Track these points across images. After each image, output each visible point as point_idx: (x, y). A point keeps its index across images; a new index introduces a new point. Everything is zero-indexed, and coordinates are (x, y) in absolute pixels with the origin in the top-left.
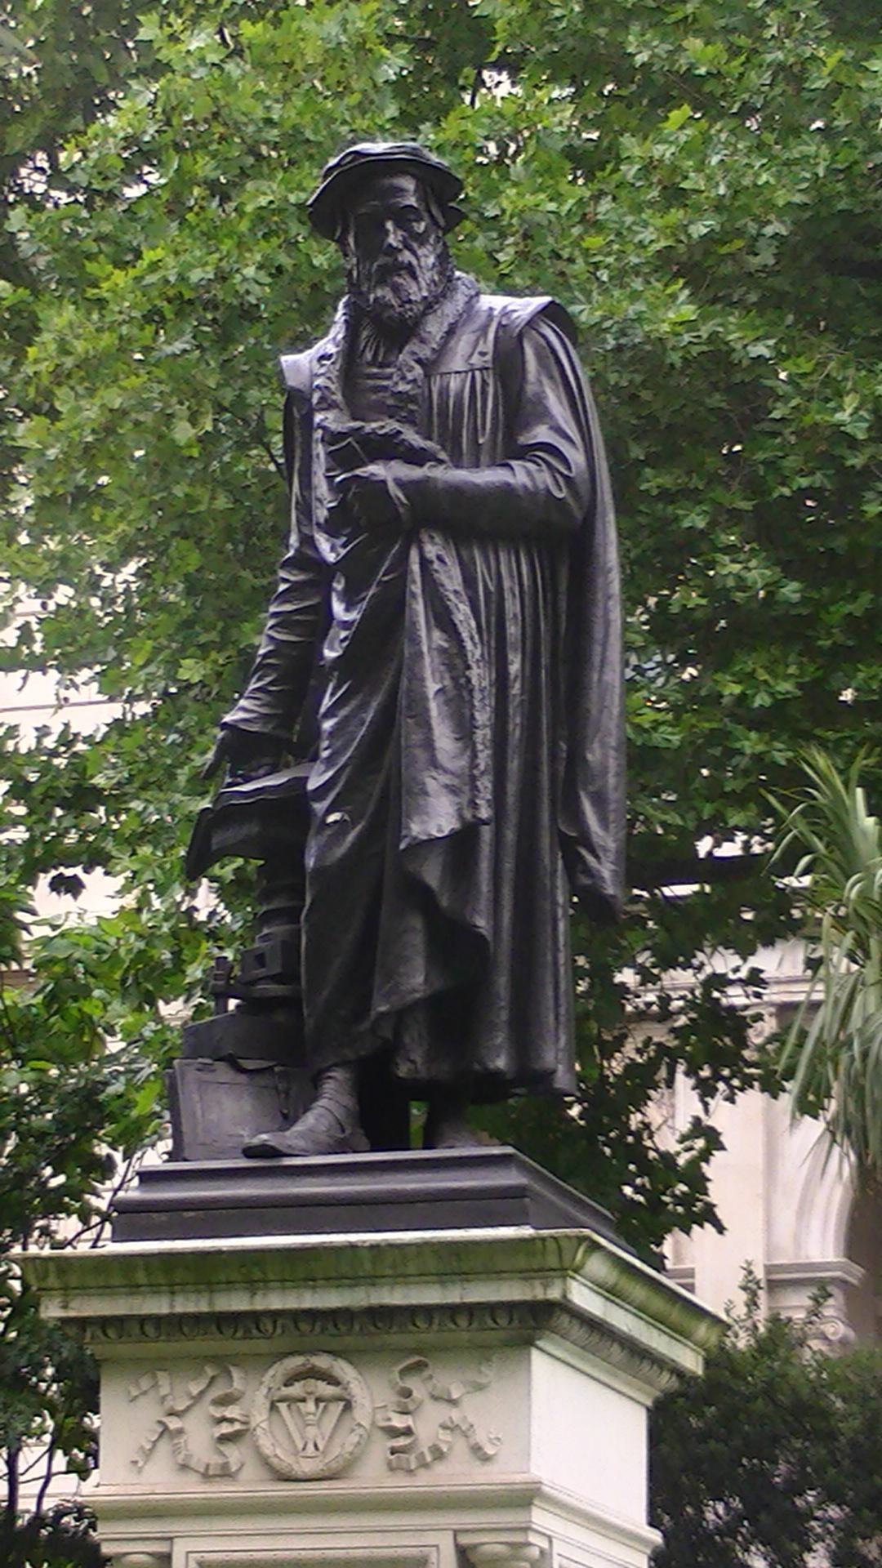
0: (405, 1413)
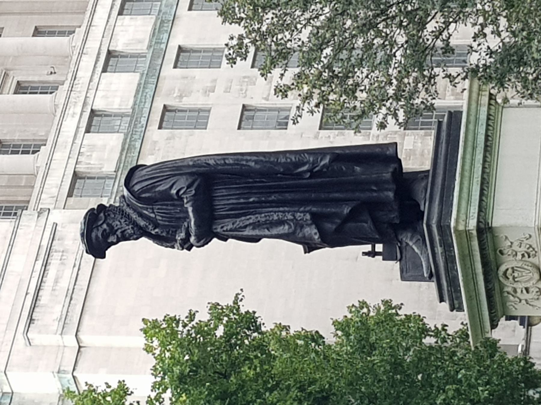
0: (516, 255)
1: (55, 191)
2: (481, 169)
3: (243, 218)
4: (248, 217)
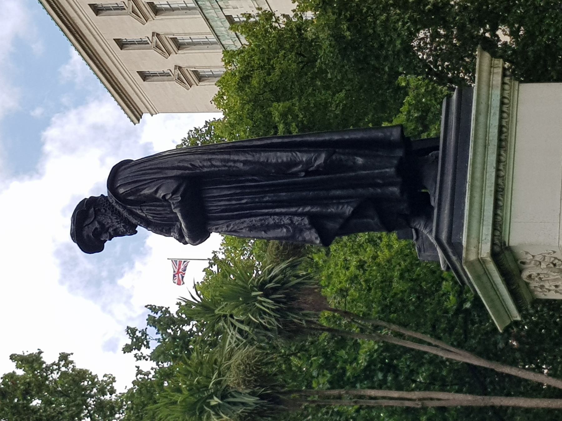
2: (494, 174)
3: (238, 221)
4: (242, 220)
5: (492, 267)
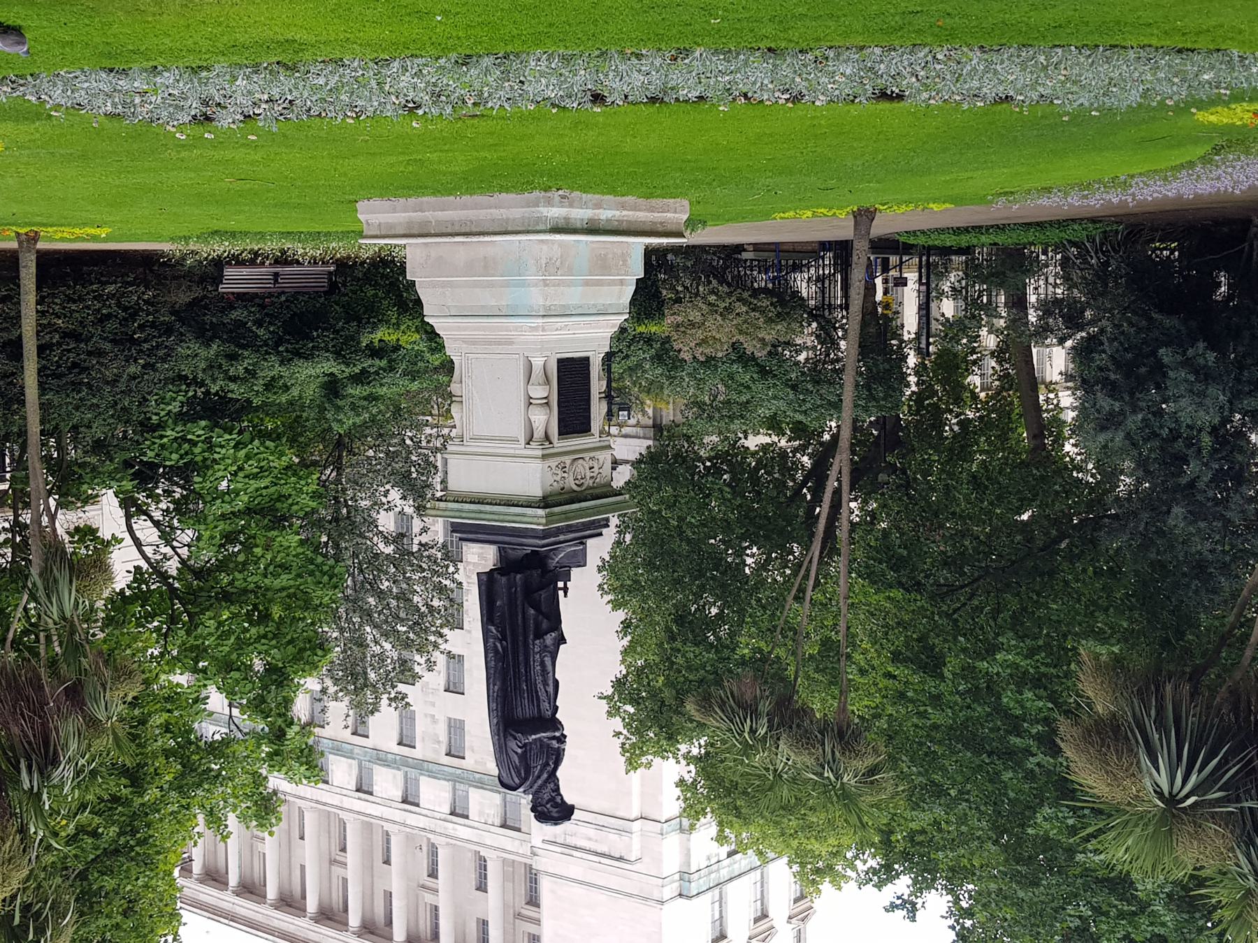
1: (517, 842)
5: (557, 509)
